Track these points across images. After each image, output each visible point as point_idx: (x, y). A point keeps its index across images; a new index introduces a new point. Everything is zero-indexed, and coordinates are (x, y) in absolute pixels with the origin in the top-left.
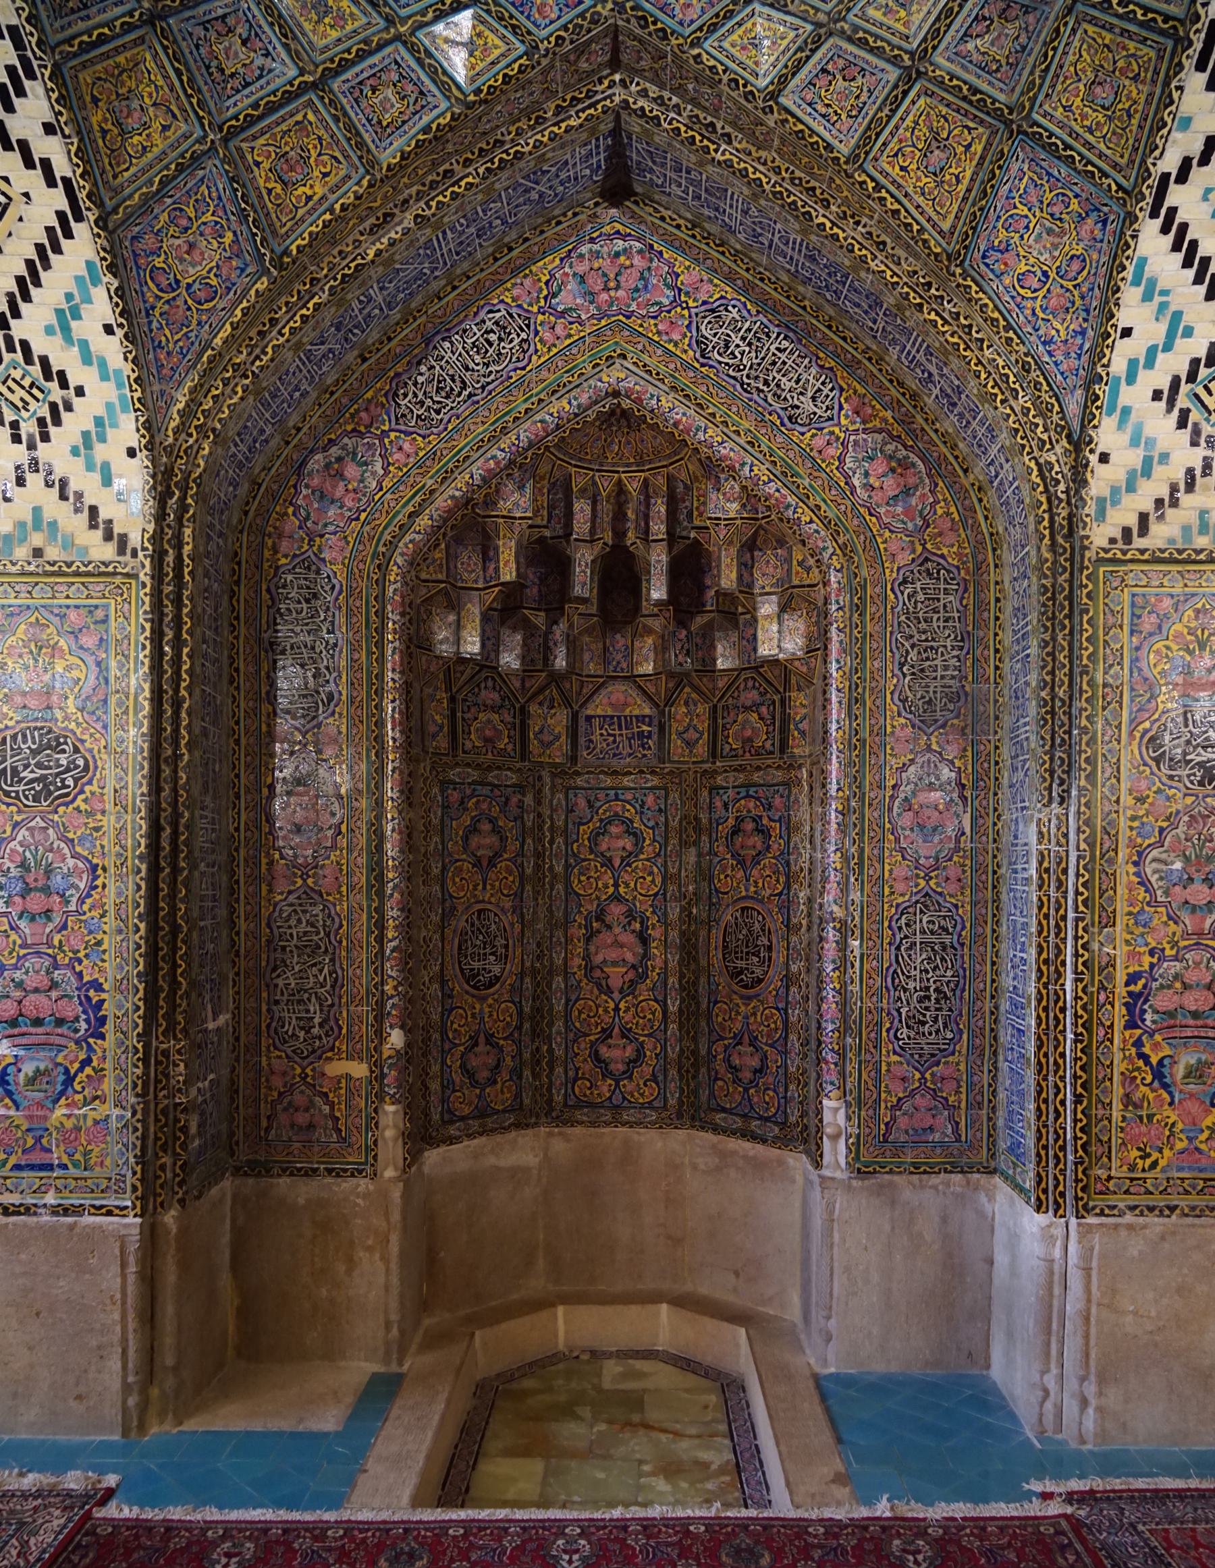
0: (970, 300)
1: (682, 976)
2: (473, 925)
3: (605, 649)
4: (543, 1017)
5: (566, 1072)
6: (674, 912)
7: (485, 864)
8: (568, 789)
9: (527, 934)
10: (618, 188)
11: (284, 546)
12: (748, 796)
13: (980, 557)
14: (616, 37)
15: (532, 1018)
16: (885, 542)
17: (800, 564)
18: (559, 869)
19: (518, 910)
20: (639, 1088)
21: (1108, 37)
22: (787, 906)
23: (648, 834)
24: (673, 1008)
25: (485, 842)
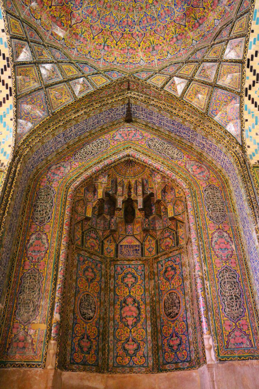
0: (210, 121)
1: (151, 320)
2: (85, 298)
3: (126, 228)
4: (106, 334)
6: (148, 301)
7: (90, 281)
9: (102, 306)
10: (129, 119)
11: (42, 184)
12: (169, 261)
13: (224, 185)
14: (129, 83)
17: (178, 192)
18: (112, 287)
20: (138, 360)
21: (229, 66)
22: (183, 288)
23: (139, 277)
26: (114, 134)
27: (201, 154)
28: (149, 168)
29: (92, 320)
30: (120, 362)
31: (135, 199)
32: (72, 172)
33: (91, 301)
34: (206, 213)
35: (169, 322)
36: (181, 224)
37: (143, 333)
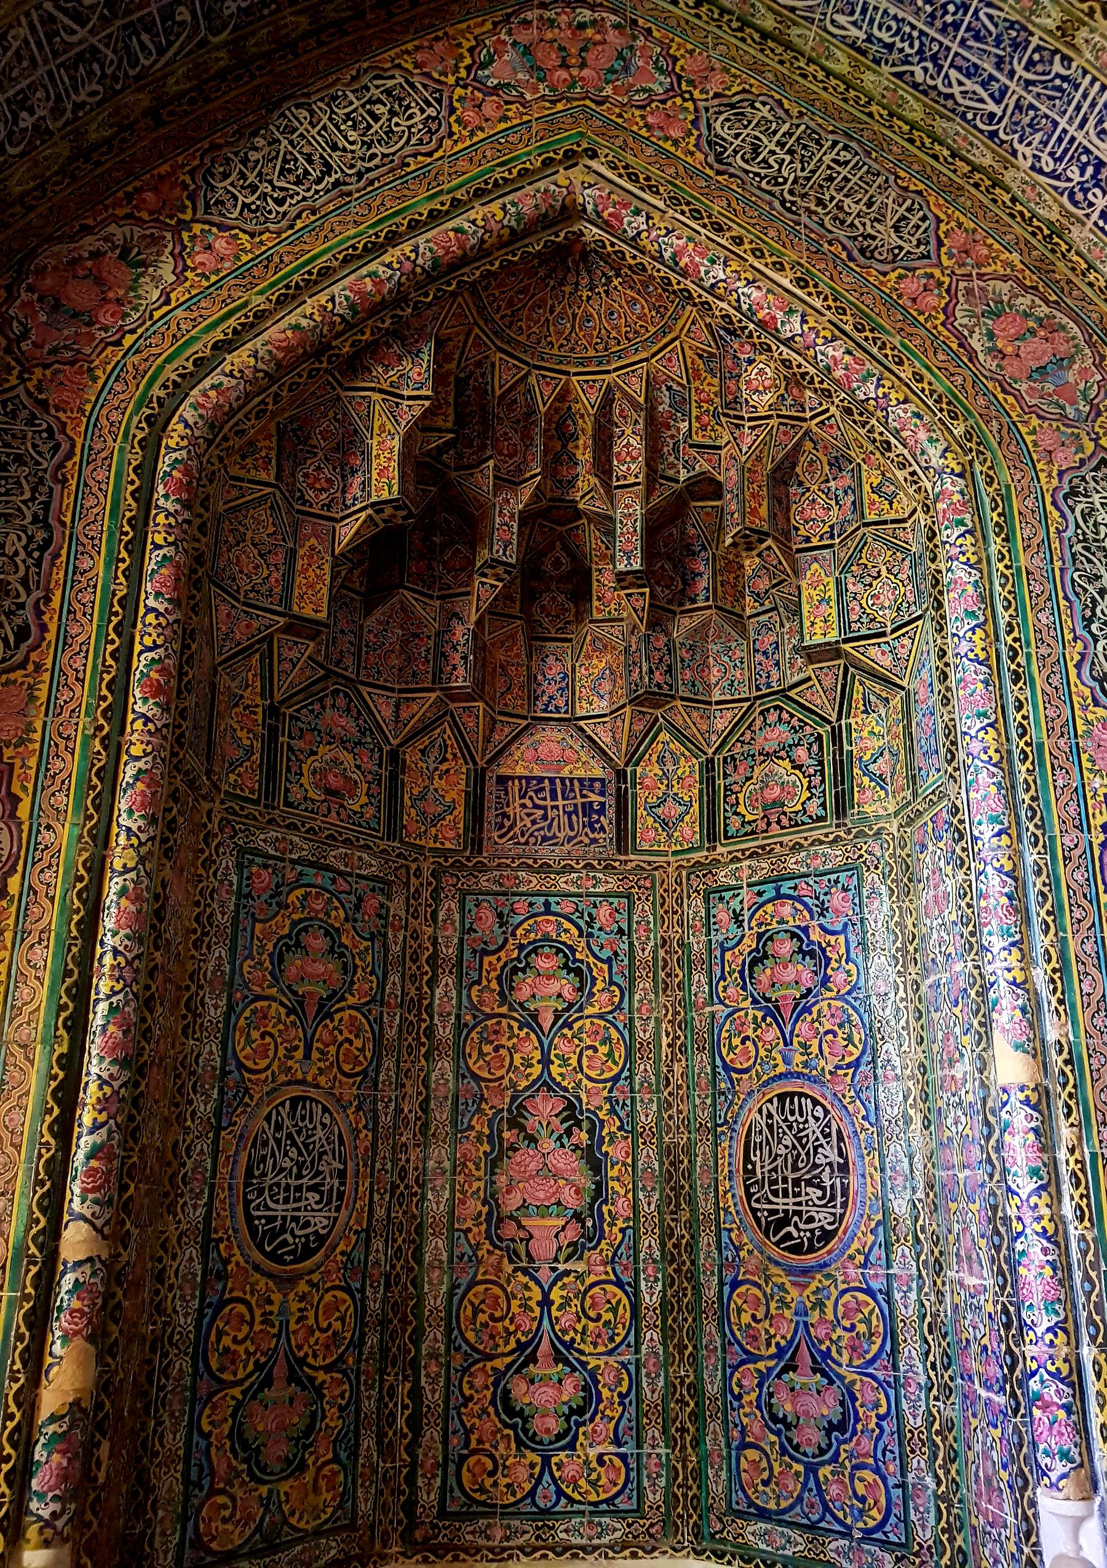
1: (667, 1233)
4: (404, 1321)
5: (445, 1441)
8: (464, 894)
9: (384, 1150)
12: (779, 896)
15: (384, 1322)
16: (1033, 432)
19: (368, 1105)
24: (650, 1298)
25: (314, 970)
26: (480, 42)
27: (1056, 231)
28: (706, 306)
29: (318, 1257)
30: (482, 1490)
31: (599, 506)
32: (188, 305)
33: (320, 1133)
34: (1073, 654)
35: (774, 1270)
36: (878, 688)
37: (614, 1310)
